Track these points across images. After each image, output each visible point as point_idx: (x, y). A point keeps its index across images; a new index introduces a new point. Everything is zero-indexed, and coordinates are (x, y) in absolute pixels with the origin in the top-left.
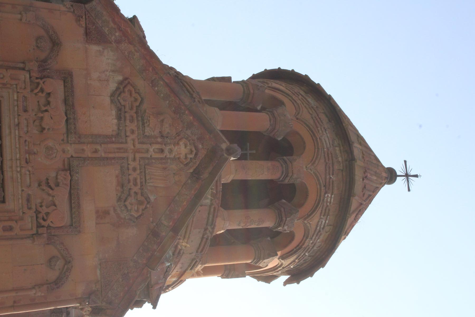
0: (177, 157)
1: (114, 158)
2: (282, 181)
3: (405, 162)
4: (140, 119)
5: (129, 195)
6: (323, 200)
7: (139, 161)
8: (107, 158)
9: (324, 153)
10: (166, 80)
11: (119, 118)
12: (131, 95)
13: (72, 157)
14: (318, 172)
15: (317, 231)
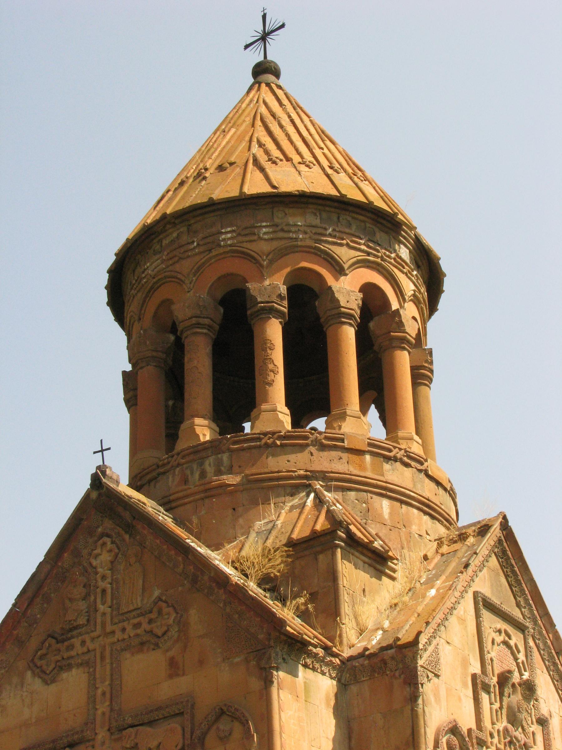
0: (110, 565)
1: (112, 664)
2: (210, 327)
3: (247, 47)
4: (69, 635)
5: (151, 632)
6: (230, 246)
7: (116, 624)
8: (112, 675)
9: (168, 267)
10: (25, 607)
11: (69, 667)
12: (45, 655)
13: (109, 730)
14: (191, 270)
15: (281, 235)
